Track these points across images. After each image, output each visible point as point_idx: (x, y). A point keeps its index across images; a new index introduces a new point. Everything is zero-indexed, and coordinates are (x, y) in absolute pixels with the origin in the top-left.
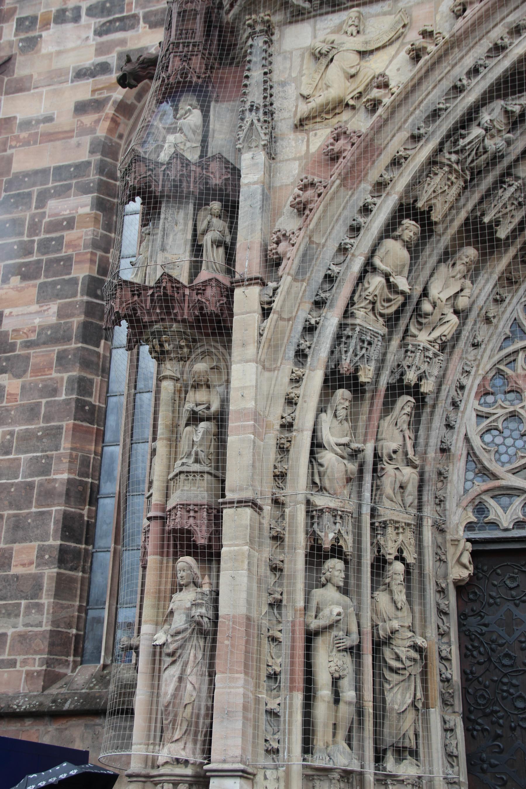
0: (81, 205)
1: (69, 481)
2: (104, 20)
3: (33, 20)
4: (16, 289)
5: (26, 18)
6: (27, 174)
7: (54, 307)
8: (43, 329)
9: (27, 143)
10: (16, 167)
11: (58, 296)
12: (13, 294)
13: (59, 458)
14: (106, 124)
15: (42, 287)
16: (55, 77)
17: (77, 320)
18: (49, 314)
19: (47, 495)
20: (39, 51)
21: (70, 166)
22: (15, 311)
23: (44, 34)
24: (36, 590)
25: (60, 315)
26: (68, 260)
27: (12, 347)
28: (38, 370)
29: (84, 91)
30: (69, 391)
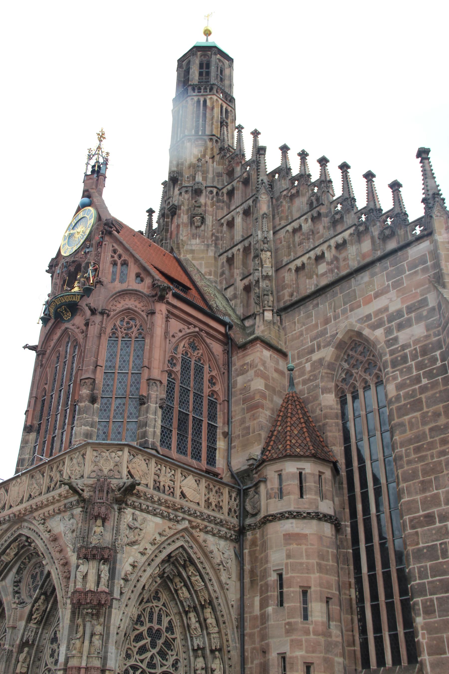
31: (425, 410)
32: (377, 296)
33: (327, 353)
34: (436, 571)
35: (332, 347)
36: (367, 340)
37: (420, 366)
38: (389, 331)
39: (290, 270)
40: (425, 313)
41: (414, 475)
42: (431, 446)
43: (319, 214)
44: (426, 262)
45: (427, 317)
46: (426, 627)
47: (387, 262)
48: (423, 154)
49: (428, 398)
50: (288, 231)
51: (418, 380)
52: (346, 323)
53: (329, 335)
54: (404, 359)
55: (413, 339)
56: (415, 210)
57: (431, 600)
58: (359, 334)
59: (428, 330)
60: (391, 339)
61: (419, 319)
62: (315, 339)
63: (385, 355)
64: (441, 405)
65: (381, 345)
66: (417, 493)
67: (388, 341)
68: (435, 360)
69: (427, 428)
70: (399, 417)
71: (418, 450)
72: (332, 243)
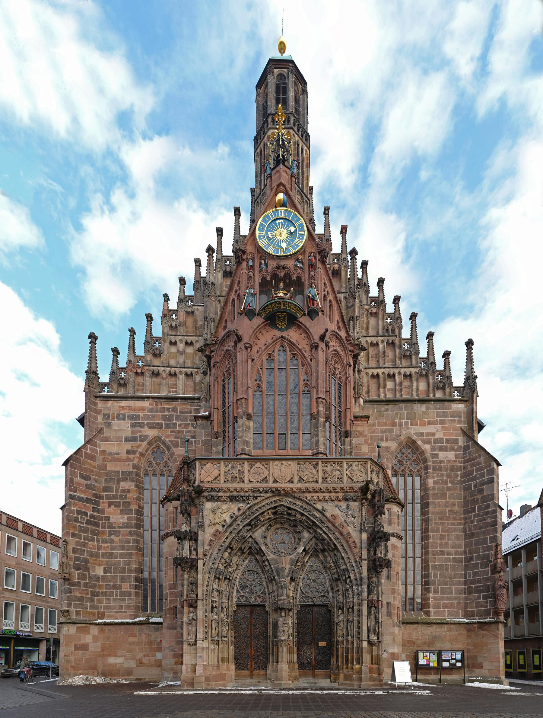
0: (131, 486)
1: (136, 567)
2: (134, 422)
3: (109, 415)
4: (113, 509)
5: (106, 414)
6: (112, 472)
7: (126, 517)
8: (123, 523)
9: (111, 461)
10: (108, 469)
11: (127, 514)
12: (112, 511)
13: (132, 561)
14: (138, 459)
15: (121, 510)
16: (118, 439)
17: (134, 522)
18: (125, 519)
19: (130, 571)
20: (112, 428)
21: (126, 472)
22: (114, 516)
23: (113, 422)
24: (130, 595)
25: (128, 520)
26: (129, 502)
27: (115, 528)
28: (123, 536)
29: (128, 446)
30: (134, 543)
31: (448, 500)
32: (429, 423)
33: (393, 445)
34: (441, 576)
35: (396, 443)
36: (418, 448)
37: (448, 476)
38: (433, 449)
39: (367, 373)
40: (456, 448)
41: (437, 530)
42: (448, 519)
43: (393, 343)
44: (460, 417)
45: (456, 450)
46: (434, 598)
47: (439, 405)
48: (469, 344)
49: (450, 494)
50: (367, 341)
51: (446, 483)
52: (407, 431)
53: (394, 434)
54: (440, 469)
55: (447, 459)
56: (458, 379)
57: (438, 588)
58: (414, 442)
59: (456, 458)
60: (434, 454)
61: (452, 449)
62: (384, 432)
63: (430, 462)
64: (456, 500)
65: (428, 455)
66: (437, 540)
67: (433, 454)
68: (457, 476)
69: (447, 509)
70: (433, 499)
71: (441, 519)
72: (403, 371)
